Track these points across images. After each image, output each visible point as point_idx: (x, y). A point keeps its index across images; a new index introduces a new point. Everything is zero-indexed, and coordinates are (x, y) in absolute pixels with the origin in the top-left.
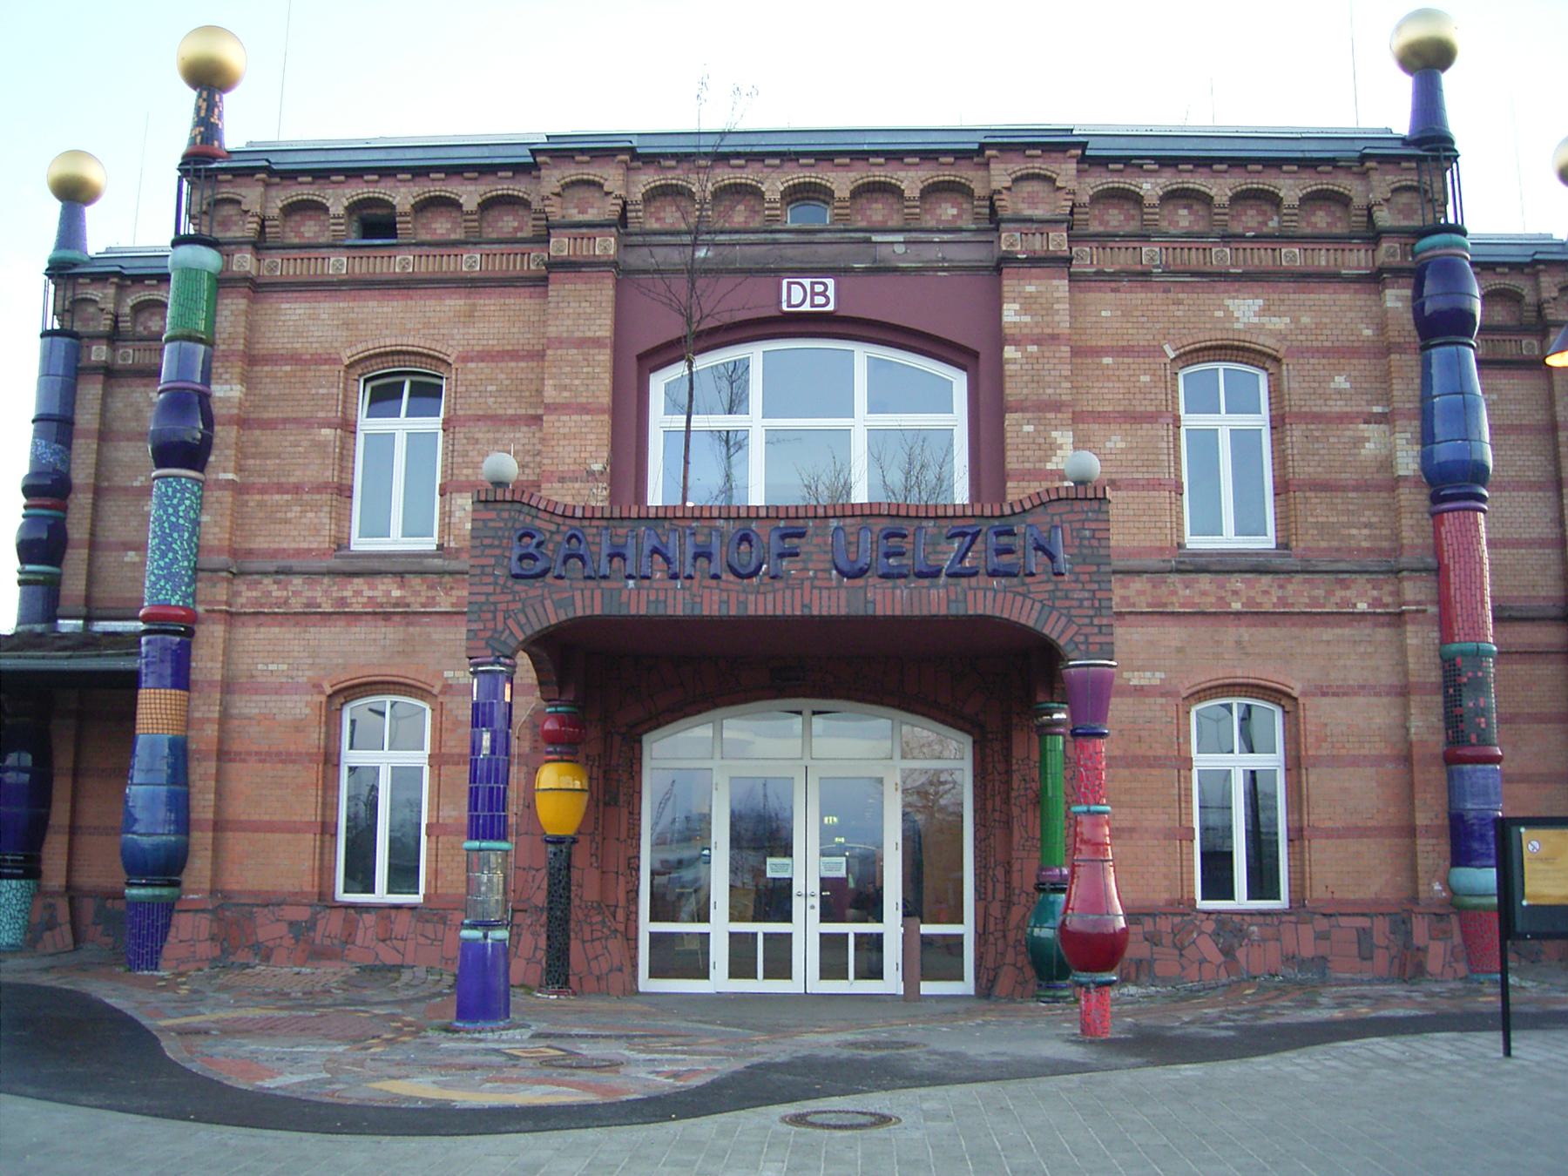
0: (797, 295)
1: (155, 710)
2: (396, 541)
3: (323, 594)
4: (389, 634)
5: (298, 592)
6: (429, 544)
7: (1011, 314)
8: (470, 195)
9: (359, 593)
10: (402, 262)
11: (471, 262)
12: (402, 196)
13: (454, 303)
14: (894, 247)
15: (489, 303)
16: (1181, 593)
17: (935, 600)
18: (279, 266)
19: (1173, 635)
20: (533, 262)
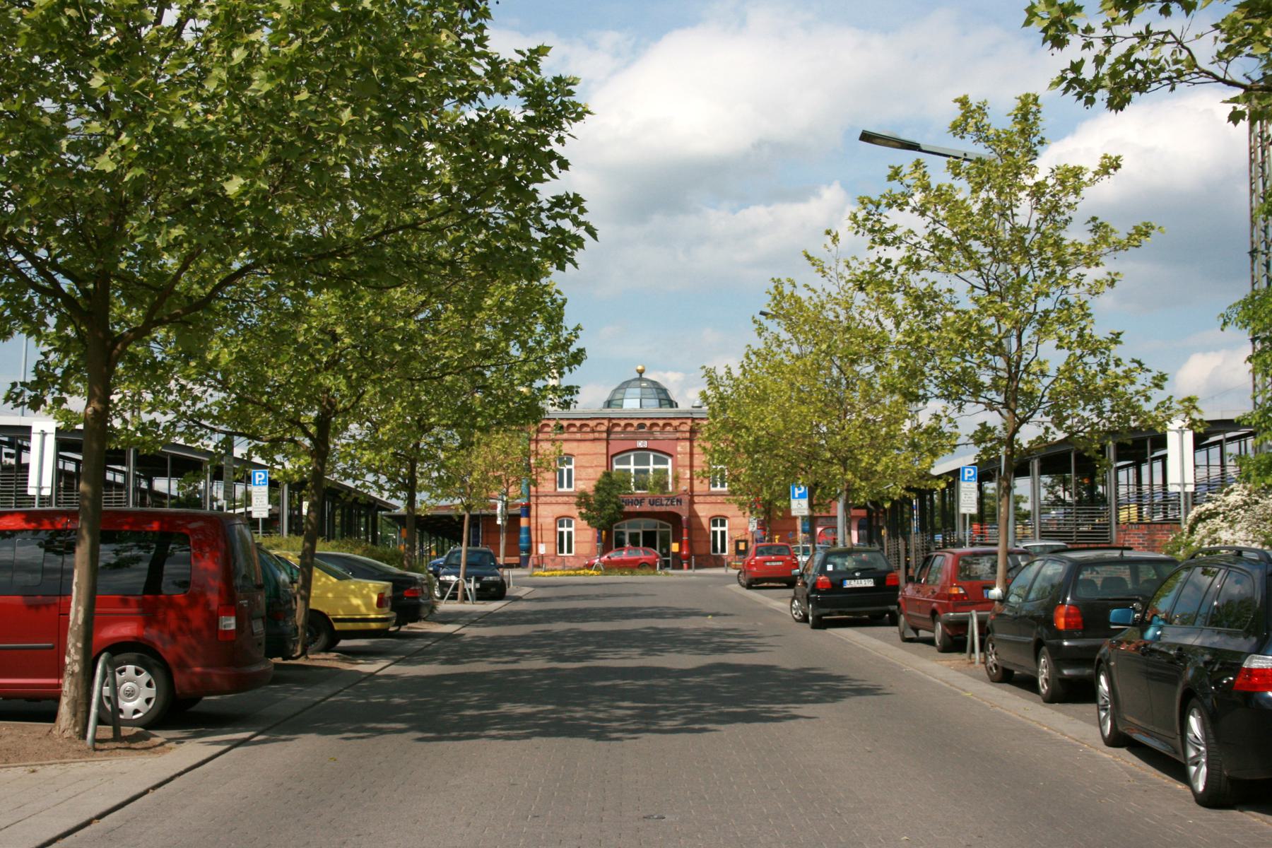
0: (640, 444)
1: (524, 522)
2: (565, 489)
3: (553, 500)
4: (566, 507)
5: (548, 499)
6: (572, 490)
7: (679, 449)
8: (578, 423)
9: (560, 499)
10: (565, 436)
11: (578, 436)
12: (565, 423)
13: (575, 444)
14: (658, 435)
15: (582, 444)
16: (709, 499)
17: (663, 509)
18: (541, 436)
19: (707, 506)
20: (591, 436)
